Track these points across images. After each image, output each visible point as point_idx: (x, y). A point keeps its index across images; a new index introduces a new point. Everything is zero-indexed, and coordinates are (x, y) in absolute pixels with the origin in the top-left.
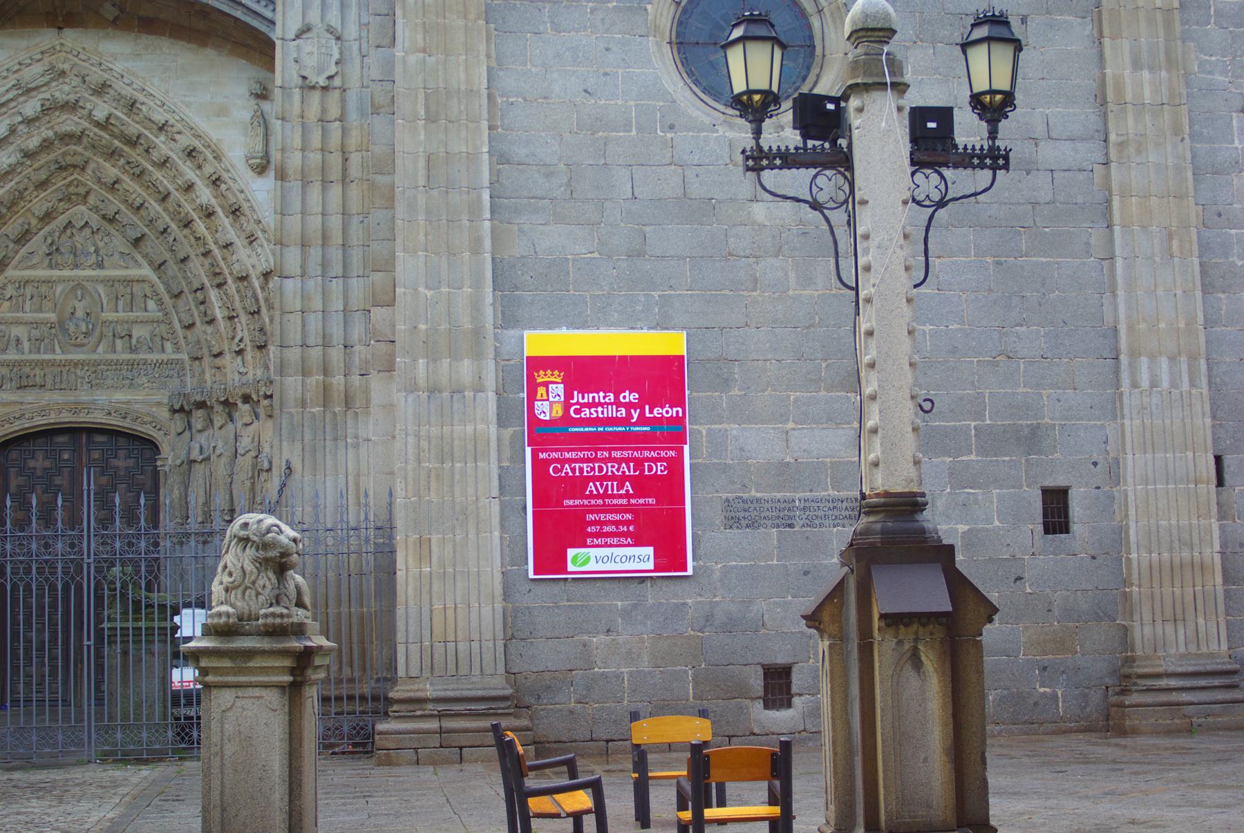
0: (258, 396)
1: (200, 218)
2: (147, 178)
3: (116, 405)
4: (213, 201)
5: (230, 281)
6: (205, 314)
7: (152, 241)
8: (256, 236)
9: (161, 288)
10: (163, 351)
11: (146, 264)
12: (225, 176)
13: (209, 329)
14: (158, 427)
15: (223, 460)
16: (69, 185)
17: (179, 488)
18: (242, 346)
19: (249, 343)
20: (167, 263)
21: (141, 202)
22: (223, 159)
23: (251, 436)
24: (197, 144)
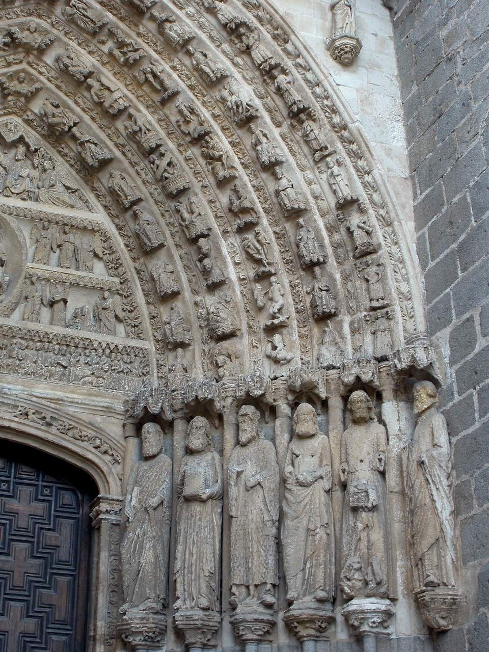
0: (328, 390)
1: (224, 129)
2: (146, 66)
3: (40, 401)
4: (257, 102)
5: (265, 221)
6: (206, 272)
7: (125, 170)
8: (330, 149)
9: (119, 242)
10: (114, 333)
11: (101, 209)
12: (288, 63)
13: (211, 301)
14: (103, 448)
15: (258, 496)
16: (11, 77)
17: (154, 547)
18: (282, 318)
19: (294, 315)
20: (143, 204)
21: (127, 104)
22: (293, 37)
23: (318, 455)
24: (249, 17)
